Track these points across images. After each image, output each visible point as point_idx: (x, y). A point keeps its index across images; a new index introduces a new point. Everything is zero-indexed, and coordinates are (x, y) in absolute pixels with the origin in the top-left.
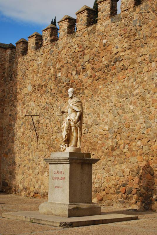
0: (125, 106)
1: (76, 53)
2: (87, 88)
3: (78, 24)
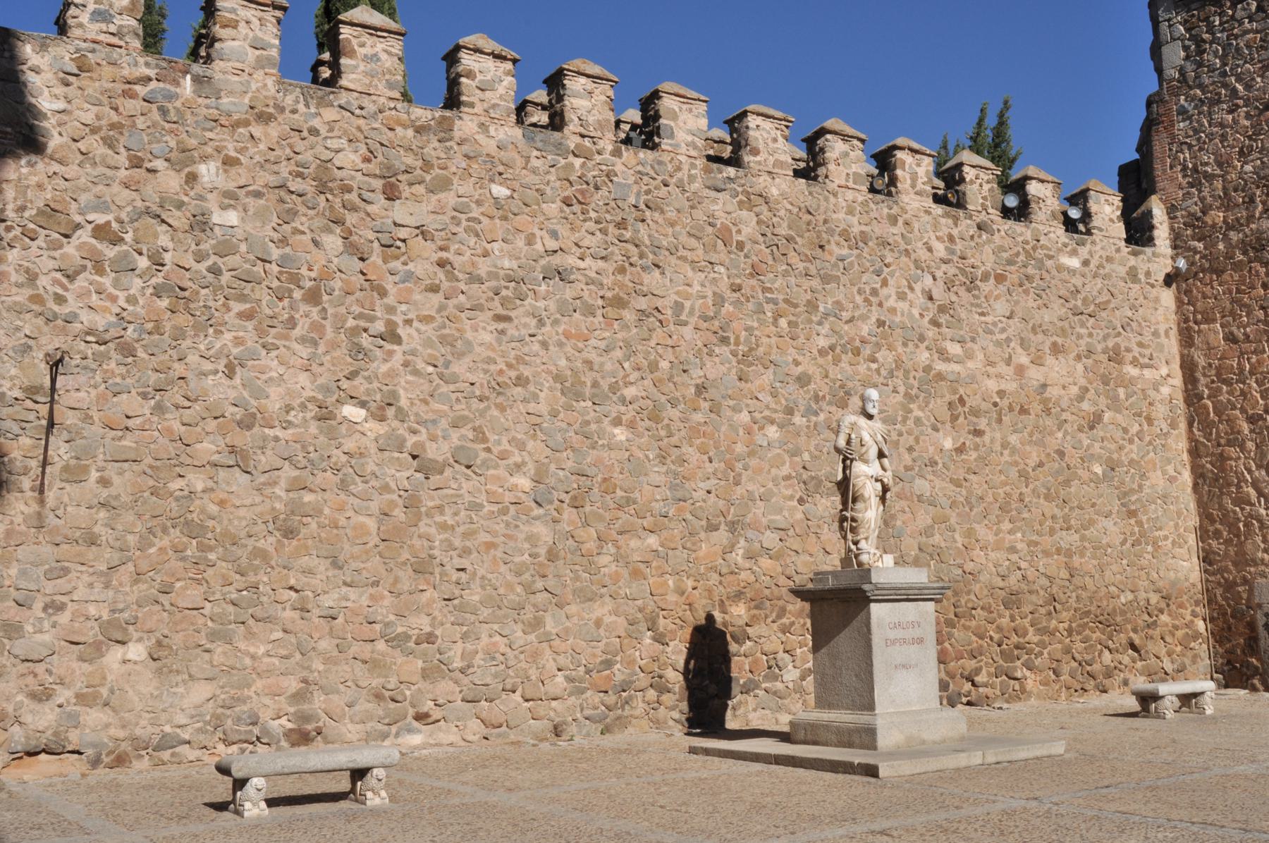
0: (594, 427)
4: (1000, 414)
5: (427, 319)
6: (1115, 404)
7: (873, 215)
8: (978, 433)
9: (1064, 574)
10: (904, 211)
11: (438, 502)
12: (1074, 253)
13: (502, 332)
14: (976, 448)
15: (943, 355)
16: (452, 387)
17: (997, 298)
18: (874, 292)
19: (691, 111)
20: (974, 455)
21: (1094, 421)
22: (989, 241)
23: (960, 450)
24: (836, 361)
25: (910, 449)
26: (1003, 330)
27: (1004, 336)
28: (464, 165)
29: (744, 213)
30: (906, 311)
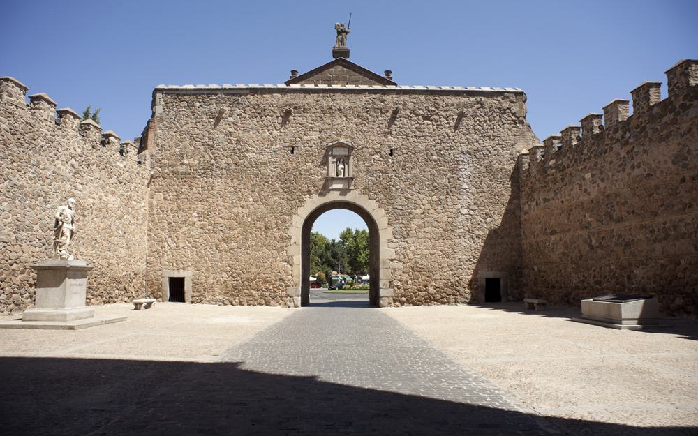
4: (92, 210)
6: (128, 213)
7: (56, 133)
8: (85, 216)
9: (107, 265)
12: (122, 163)
15: (76, 188)
21: (121, 218)
22: (96, 152)
24: (35, 183)
26: (97, 183)
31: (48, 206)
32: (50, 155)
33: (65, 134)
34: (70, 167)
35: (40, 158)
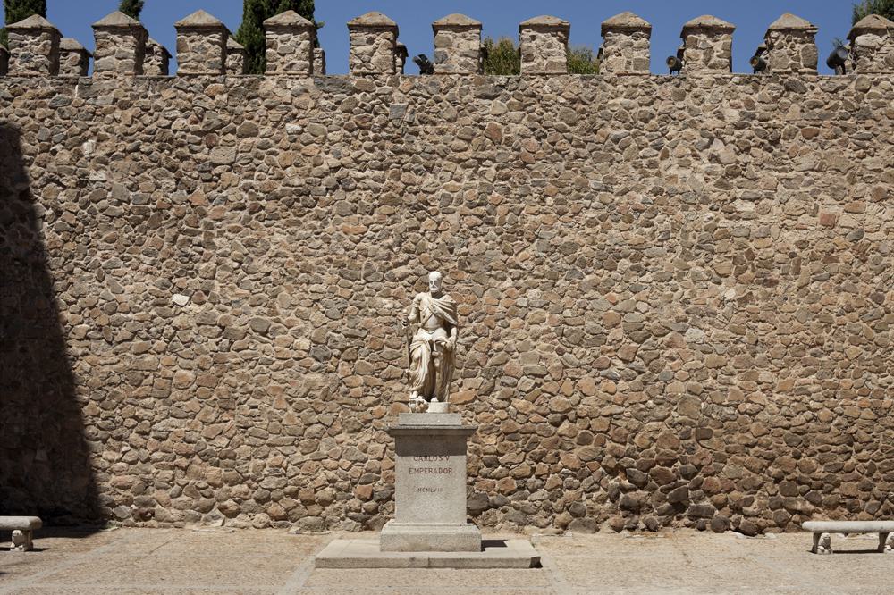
1: (175, 131)
2: (227, 233)
3: (185, 54)
5: (236, 230)
8: (774, 283)
10: (693, 86)
11: (239, 359)
13: (292, 233)
14: (767, 297)
15: (732, 214)
16: (252, 277)
17: (802, 153)
18: (653, 165)
19: (464, 37)
20: (762, 304)
23: (743, 301)
25: (685, 302)
26: (811, 183)
27: (810, 189)
28: (265, 113)
29: (514, 114)
30: (688, 176)
31: (648, 277)
32: (641, 153)
33: (686, 86)
34: (705, 165)
35: (611, 171)
